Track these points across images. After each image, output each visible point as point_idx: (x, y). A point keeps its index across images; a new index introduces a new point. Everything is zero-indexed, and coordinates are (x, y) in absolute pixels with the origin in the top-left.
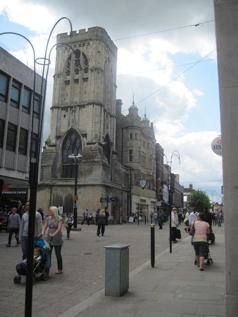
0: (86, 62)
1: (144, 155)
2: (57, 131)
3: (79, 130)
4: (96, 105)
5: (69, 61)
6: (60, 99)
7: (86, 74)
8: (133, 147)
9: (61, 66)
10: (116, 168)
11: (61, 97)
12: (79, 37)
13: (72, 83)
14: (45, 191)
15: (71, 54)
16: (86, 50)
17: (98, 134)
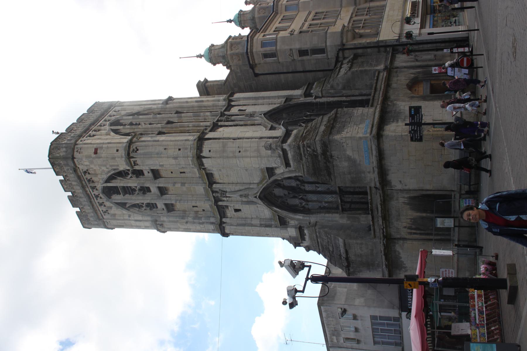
0: (122, 174)
1: (311, 17)
2: (270, 226)
3: (261, 182)
4: (201, 151)
5: (127, 206)
6: (203, 220)
7: (146, 173)
8: (291, 50)
9: (140, 221)
10: (340, 87)
11: (200, 218)
12: (77, 191)
13: (169, 199)
14: (401, 251)
15: (112, 203)
16: (99, 176)
17: (263, 143)
